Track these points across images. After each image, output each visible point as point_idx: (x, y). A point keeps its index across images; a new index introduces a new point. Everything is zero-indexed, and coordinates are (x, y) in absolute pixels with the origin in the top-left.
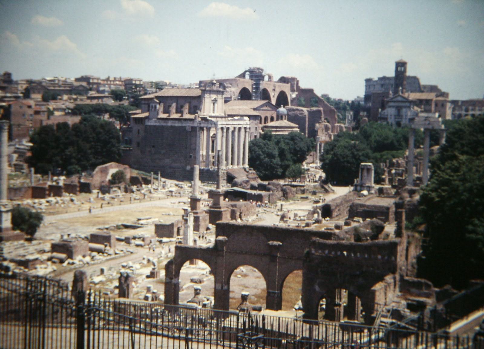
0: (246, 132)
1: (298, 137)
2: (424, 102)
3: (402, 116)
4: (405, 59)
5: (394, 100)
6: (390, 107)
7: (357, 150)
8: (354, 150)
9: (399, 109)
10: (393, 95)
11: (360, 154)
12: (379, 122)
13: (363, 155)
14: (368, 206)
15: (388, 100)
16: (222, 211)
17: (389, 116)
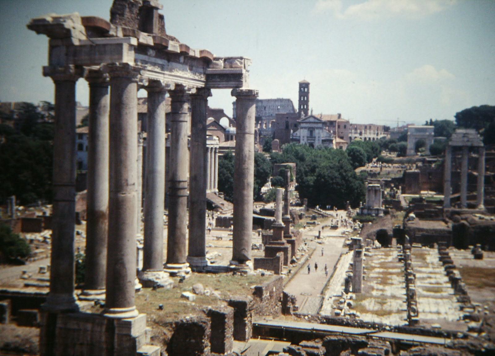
0: (215, 153)
1: (260, 158)
2: (328, 124)
3: (315, 137)
4: (308, 80)
5: (306, 121)
6: (302, 128)
7: (345, 171)
8: (342, 171)
9: (311, 130)
10: (305, 116)
11: (349, 175)
12: (291, 143)
13: (351, 176)
14: (427, 230)
15: (300, 121)
16: (294, 241)
17: (302, 138)
